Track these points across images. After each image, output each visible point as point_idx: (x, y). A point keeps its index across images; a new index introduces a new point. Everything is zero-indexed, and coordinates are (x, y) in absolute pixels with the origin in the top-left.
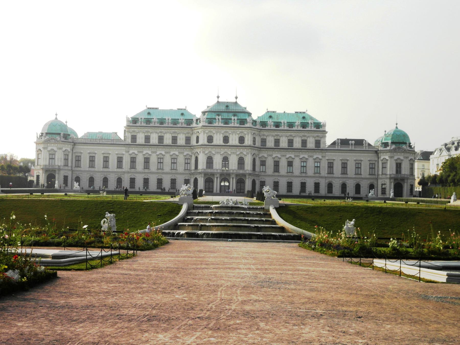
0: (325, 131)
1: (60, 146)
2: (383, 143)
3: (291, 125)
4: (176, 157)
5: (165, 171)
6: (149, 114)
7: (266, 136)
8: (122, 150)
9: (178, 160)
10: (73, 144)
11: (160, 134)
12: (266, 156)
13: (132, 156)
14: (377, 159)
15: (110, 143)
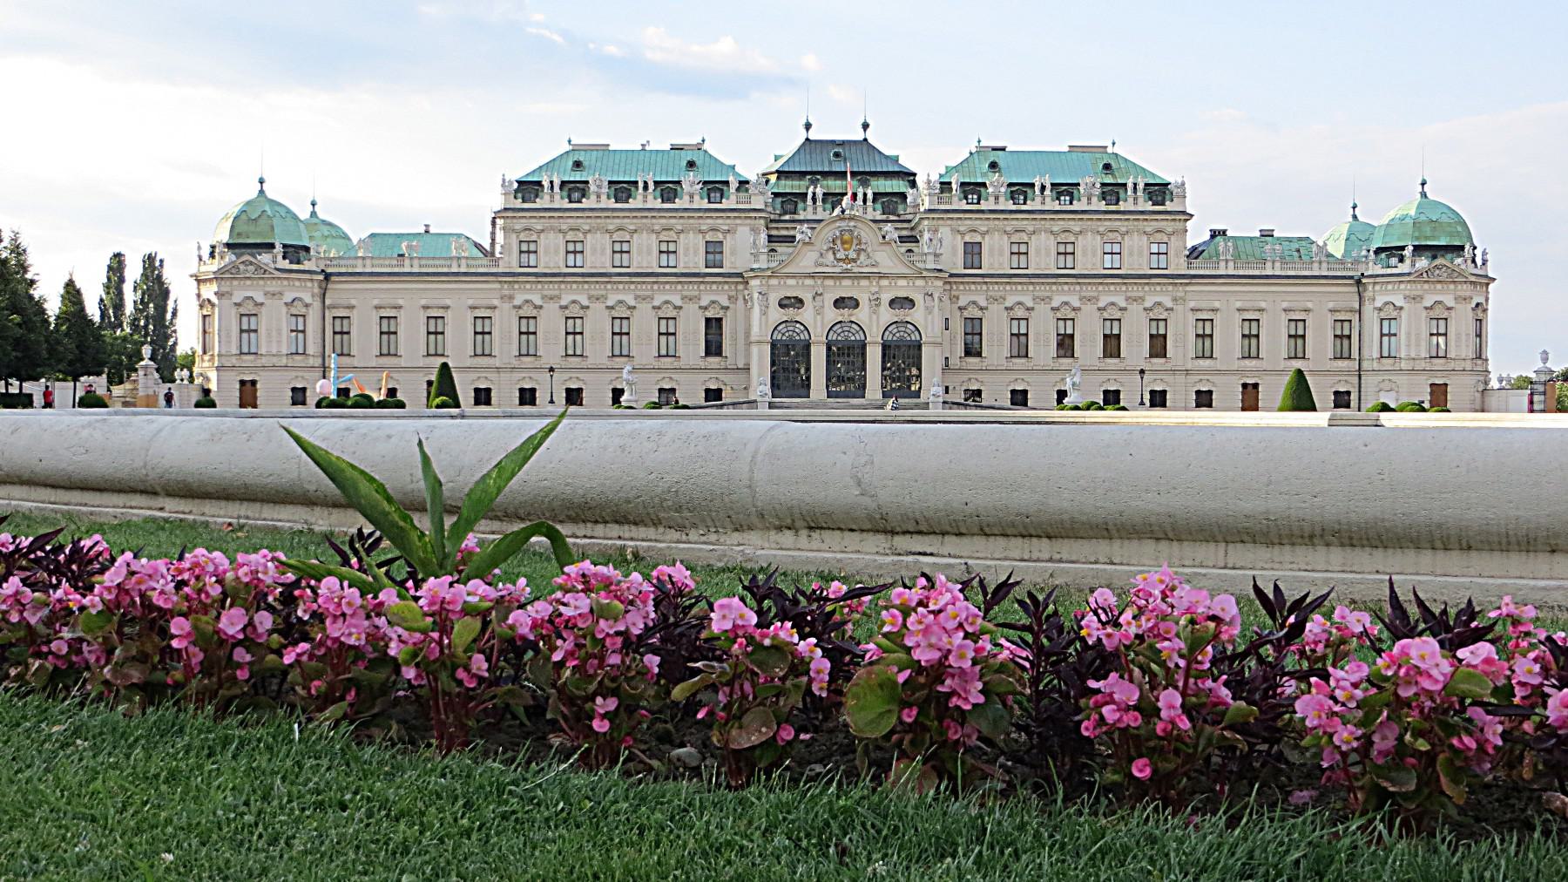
0: (1183, 213)
1: (273, 286)
2: (1378, 251)
3: (1065, 190)
4: (673, 314)
5: (637, 362)
6: (578, 164)
7: (983, 234)
8: (488, 293)
9: (681, 323)
10: (321, 277)
11: (615, 237)
12: (983, 303)
13: (522, 313)
14: (1357, 306)
15: (445, 270)
